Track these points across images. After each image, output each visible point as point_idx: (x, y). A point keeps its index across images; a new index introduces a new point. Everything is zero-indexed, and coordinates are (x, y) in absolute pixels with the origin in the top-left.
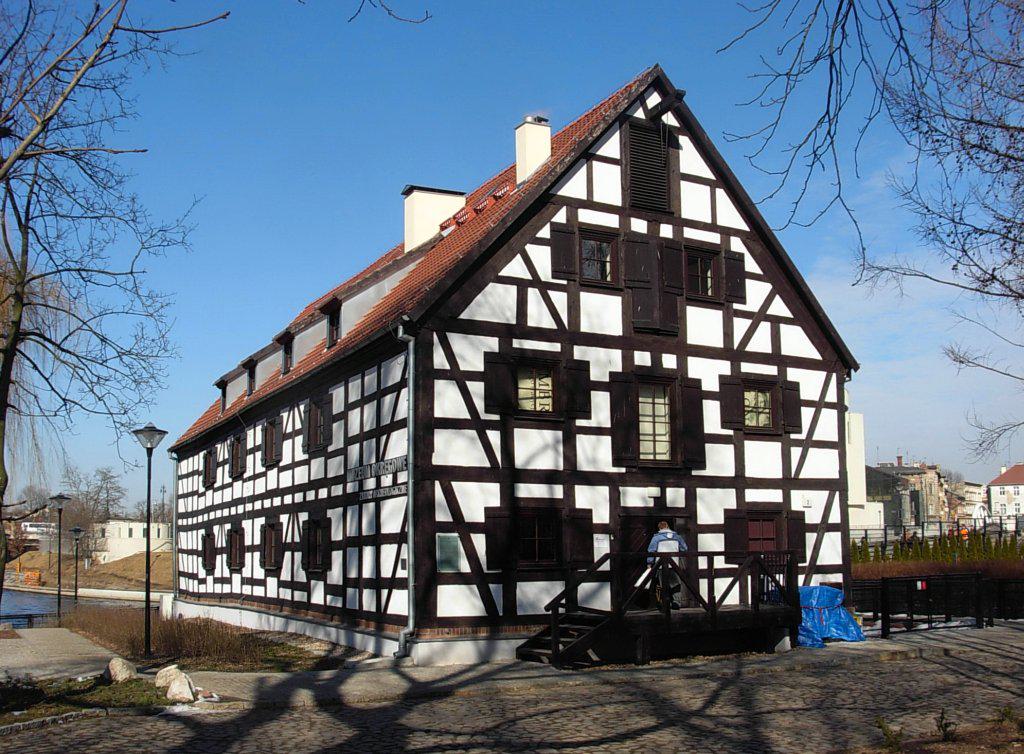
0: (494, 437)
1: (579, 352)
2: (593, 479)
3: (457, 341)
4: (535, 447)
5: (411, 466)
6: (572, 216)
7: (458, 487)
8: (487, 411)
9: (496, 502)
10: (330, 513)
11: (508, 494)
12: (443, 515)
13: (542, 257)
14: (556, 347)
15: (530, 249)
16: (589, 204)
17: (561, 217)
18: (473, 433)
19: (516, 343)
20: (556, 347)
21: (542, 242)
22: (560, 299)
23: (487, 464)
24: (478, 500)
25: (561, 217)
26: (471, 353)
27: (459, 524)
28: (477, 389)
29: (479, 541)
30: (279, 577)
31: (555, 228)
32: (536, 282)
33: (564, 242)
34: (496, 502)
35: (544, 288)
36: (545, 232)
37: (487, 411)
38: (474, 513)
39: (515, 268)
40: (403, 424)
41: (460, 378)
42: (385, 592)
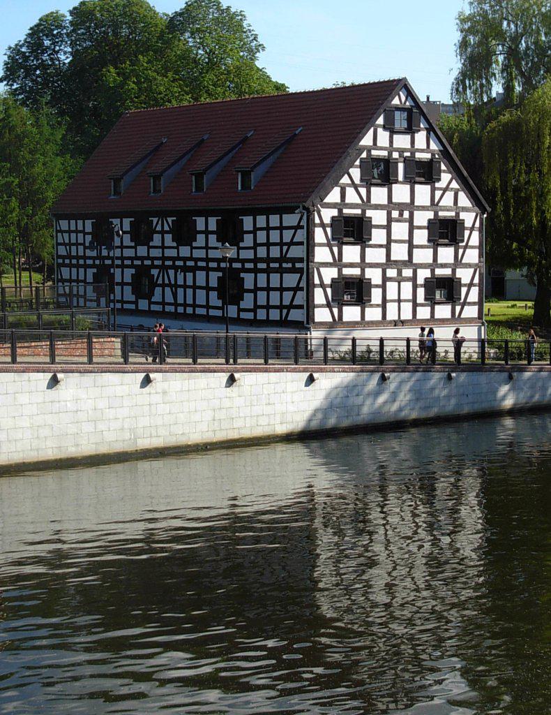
0: (335, 249)
1: (369, 213)
3: (321, 209)
4: (351, 253)
5: (305, 262)
6: (369, 151)
7: (322, 270)
8: (333, 239)
9: (336, 276)
10: (242, 275)
11: (340, 271)
12: (317, 281)
13: (356, 173)
15: (351, 170)
17: (364, 155)
18: (327, 249)
19: (346, 211)
20: (359, 211)
21: (356, 167)
23: (332, 261)
24: (329, 274)
25: (364, 155)
26: (328, 215)
27: (322, 285)
28: (329, 230)
29: (329, 291)
30: (238, 305)
31: (361, 159)
34: (336, 276)
35: (356, 187)
37: (333, 239)
38: (327, 281)
39: (345, 180)
40: (301, 243)
41: (323, 225)
42: (285, 311)
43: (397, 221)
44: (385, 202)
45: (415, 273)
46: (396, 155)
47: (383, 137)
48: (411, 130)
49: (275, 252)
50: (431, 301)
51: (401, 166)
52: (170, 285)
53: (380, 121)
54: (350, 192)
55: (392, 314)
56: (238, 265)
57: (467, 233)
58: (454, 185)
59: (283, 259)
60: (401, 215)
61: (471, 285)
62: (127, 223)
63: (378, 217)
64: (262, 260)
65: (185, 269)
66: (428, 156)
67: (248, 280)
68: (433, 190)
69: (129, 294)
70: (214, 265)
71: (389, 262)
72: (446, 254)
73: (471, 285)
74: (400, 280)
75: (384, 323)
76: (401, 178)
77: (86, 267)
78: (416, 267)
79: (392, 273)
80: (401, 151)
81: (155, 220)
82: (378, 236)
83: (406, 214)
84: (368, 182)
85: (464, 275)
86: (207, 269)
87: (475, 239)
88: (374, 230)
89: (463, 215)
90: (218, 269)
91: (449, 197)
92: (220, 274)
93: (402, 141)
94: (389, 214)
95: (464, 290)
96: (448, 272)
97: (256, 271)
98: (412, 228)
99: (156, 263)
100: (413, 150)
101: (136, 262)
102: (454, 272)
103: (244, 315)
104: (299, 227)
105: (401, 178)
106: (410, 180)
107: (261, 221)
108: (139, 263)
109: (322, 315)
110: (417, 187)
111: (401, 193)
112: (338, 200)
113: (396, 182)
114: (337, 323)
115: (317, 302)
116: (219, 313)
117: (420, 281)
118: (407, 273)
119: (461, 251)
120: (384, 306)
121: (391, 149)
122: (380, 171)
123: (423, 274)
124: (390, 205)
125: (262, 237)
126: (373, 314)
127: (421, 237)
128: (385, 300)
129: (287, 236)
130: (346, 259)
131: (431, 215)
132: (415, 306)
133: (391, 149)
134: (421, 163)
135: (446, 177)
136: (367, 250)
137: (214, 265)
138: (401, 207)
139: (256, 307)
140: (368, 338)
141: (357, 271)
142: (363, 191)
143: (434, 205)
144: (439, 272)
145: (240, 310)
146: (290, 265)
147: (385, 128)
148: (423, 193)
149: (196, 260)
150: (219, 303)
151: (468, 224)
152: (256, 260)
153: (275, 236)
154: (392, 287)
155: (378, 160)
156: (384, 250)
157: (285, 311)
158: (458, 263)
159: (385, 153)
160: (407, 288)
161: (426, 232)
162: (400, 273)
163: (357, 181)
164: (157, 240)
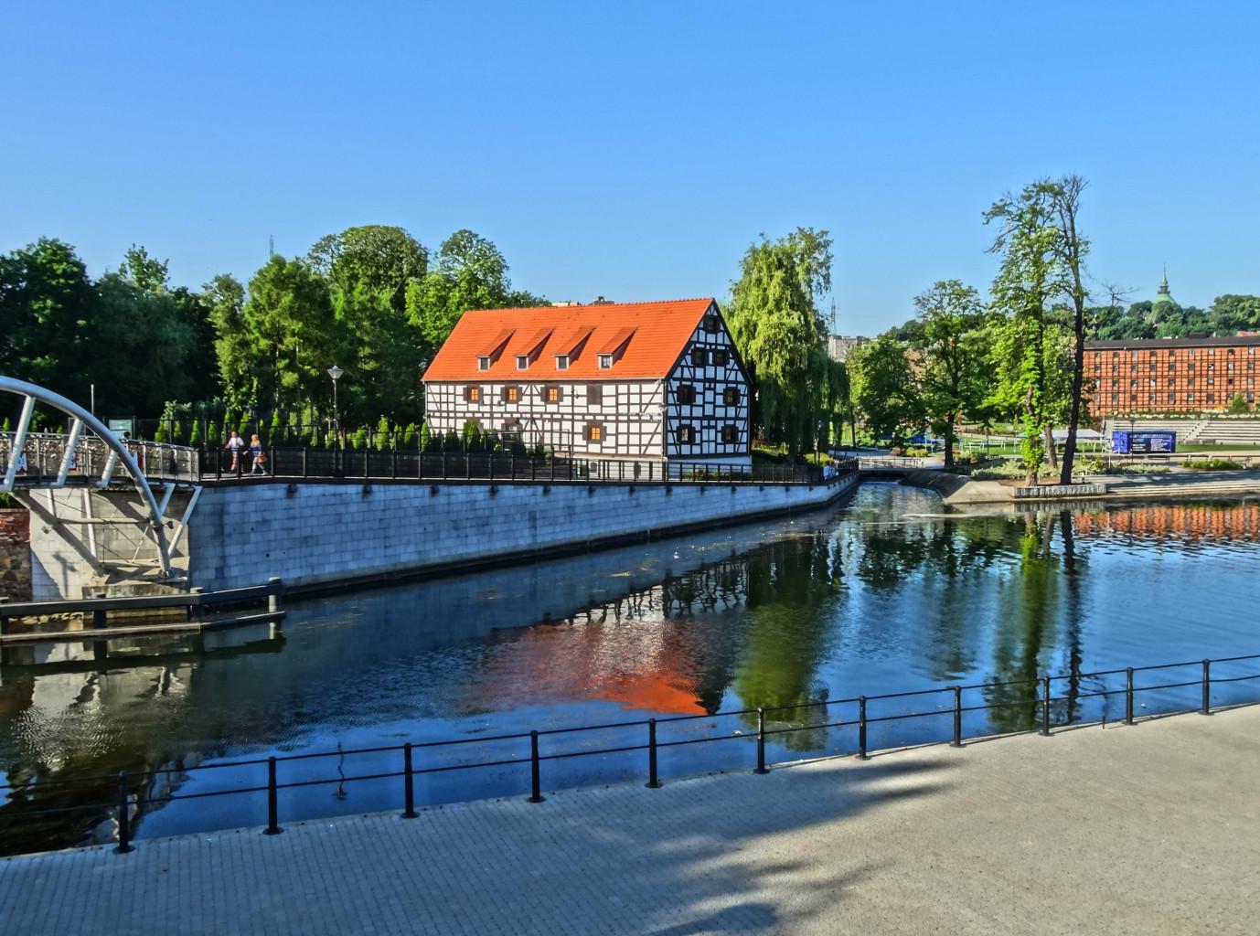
1: (695, 384)
2: (696, 418)
4: (686, 410)
10: (605, 424)
13: (689, 358)
14: (689, 383)
16: (698, 342)
19: (684, 383)
20: (689, 383)
22: (692, 370)
24: (675, 424)
26: (675, 385)
32: (687, 366)
35: (689, 367)
38: (675, 429)
39: (683, 363)
42: (643, 448)
48: (715, 331)
49: (634, 409)
51: (711, 354)
52: (537, 431)
53: (701, 326)
54: (686, 370)
56: (603, 418)
58: (736, 367)
61: (742, 432)
62: (497, 389)
63: (699, 387)
64: (622, 415)
65: (552, 420)
66: (723, 348)
67: (611, 428)
68: (726, 370)
70: (581, 417)
71: (705, 417)
72: (731, 412)
73: (742, 432)
74: (709, 427)
76: (711, 362)
77: (456, 418)
78: (717, 419)
79: (705, 423)
80: (711, 344)
81: (524, 387)
82: (699, 399)
83: (712, 385)
84: (695, 365)
85: (740, 425)
86: (573, 420)
87: (745, 401)
90: (583, 420)
91: (733, 373)
92: (585, 424)
93: (711, 338)
96: (731, 422)
97: (617, 421)
98: (715, 394)
99: (486, 415)
100: (716, 344)
101: (505, 415)
103: (605, 451)
104: (656, 393)
105: (711, 362)
106: (716, 364)
107: (623, 388)
108: (509, 416)
111: (710, 372)
116: (584, 450)
118: (712, 423)
120: (701, 445)
123: (720, 424)
124: (705, 380)
125: (623, 399)
127: (720, 400)
128: (702, 441)
129: (646, 399)
130: (683, 414)
131: (724, 386)
132: (717, 444)
133: (705, 343)
135: (732, 361)
136: (694, 408)
137: (581, 417)
139: (617, 445)
143: (726, 381)
144: (729, 422)
145: (602, 447)
146: (648, 418)
148: (721, 370)
149: (563, 414)
150: (584, 443)
152: (617, 414)
153: (635, 399)
157: (643, 448)
158: (737, 418)
159: (702, 346)
160: (712, 432)
163: (690, 364)
164: (526, 400)
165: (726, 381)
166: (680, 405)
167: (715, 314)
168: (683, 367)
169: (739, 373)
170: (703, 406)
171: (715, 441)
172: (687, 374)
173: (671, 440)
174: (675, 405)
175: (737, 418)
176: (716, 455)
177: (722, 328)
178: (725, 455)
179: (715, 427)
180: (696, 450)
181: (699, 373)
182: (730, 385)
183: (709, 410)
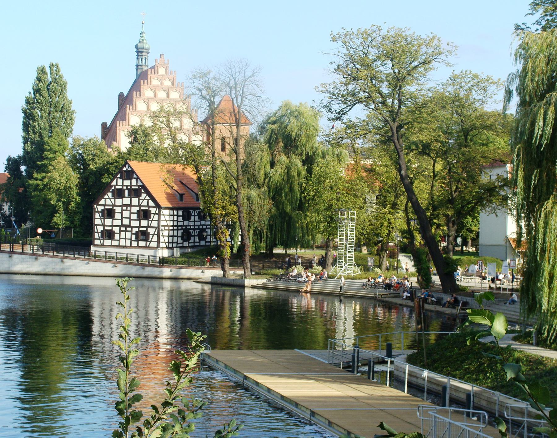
0: (103, 220)
1: (115, 208)
4: (108, 222)
11: (104, 228)
12: (96, 231)
13: (110, 194)
16: (117, 185)
19: (106, 207)
20: (111, 207)
24: (100, 229)
25: (113, 188)
26: (100, 208)
27: (97, 232)
28: (100, 214)
29: (100, 234)
33: (113, 192)
36: (111, 191)
38: (99, 231)
39: (106, 196)
41: (98, 212)
43: (124, 210)
44: (121, 204)
45: (132, 229)
46: (125, 188)
47: (120, 182)
50: (138, 239)
51: (126, 192)
54: (108, 201)
55: (122, 243)
57: (152, 215)
58: (148, 198)
59: (177, 226)
60: (127, 208)
61: (153, 235)
66: (137, 187)
68: (139, 200)
69: (197, 239)
71: (123, 226)
72: (144, 223)
73: (153, 235)
74: (126, 231)
75: (119, 246)
78: (132, 227)
79: (123, 229)
80: (127, 186)
82: (118, 216)
84: (114, 197)
85: (151, 231)
87: (156, 218)
88: (116, 214)
89: (151, 209)
93: (127, 183)
94: (122, 208)
95: (151, 236)
96: (145, 229)
98: (131, 213)
100: (131, 186)
102: (147, 229)
106: (130, 196)
109: (97, 242)
110: (133, 199)
111: (127, 201)
112: (104, 204)
113: (125, 197)
114: (103, 245)
115: (96, 238)
117: (134, 232)
118: (129, 229)
119: (150, 222)
120: (119, 240)
121: (123, 186)
122: (119, 194)
123: (135, 230)
124: (123, 205)
126: (115, 243)
127: (134, 216)
128: (120, 238)
131: (138, 209)
132: (132, 241)
133: (123, 186)
134: (134, 190)
135: (144, 195)
138: (127, 206)
140: (111, 252)
141: (110, 228)
142: (113, 200)
143: (139, 206)
147: (121, 178)
148: (135, 201)
151: (153, 212)
154: (123, 234)
155: (118, 189)
156: (120, 221)
158: (149, 227)
159: (121, 187)
160: (128, 235)
161: (136, 215)
162: (126, 229)
163: (110, 197)
165: (139, 206)
166: (104, 219)
167: (130, 169)
168: (105, 199)
169: (151, 202)
170: (122, 220)
171: (131, 239)
172: (109, 202)
173: (96, 236)
174: (100, 218)
175: (149, 227)
176: (131, 247)
177: (135, 176)
178: (138, 247)
179: (131, 231)
180: (115, 243)
181: (118, 202)
182: (142, 208)
183: (126, 222)
